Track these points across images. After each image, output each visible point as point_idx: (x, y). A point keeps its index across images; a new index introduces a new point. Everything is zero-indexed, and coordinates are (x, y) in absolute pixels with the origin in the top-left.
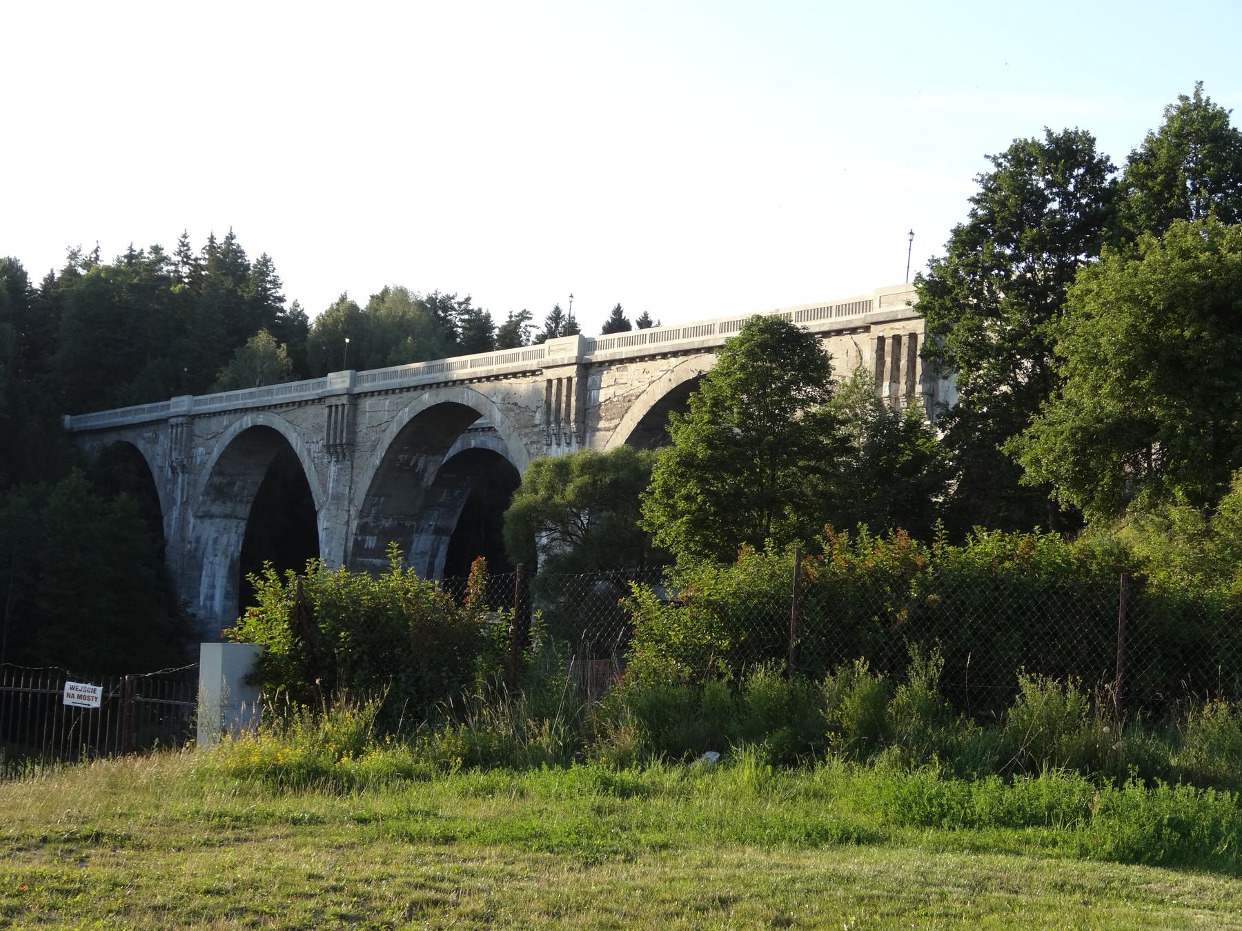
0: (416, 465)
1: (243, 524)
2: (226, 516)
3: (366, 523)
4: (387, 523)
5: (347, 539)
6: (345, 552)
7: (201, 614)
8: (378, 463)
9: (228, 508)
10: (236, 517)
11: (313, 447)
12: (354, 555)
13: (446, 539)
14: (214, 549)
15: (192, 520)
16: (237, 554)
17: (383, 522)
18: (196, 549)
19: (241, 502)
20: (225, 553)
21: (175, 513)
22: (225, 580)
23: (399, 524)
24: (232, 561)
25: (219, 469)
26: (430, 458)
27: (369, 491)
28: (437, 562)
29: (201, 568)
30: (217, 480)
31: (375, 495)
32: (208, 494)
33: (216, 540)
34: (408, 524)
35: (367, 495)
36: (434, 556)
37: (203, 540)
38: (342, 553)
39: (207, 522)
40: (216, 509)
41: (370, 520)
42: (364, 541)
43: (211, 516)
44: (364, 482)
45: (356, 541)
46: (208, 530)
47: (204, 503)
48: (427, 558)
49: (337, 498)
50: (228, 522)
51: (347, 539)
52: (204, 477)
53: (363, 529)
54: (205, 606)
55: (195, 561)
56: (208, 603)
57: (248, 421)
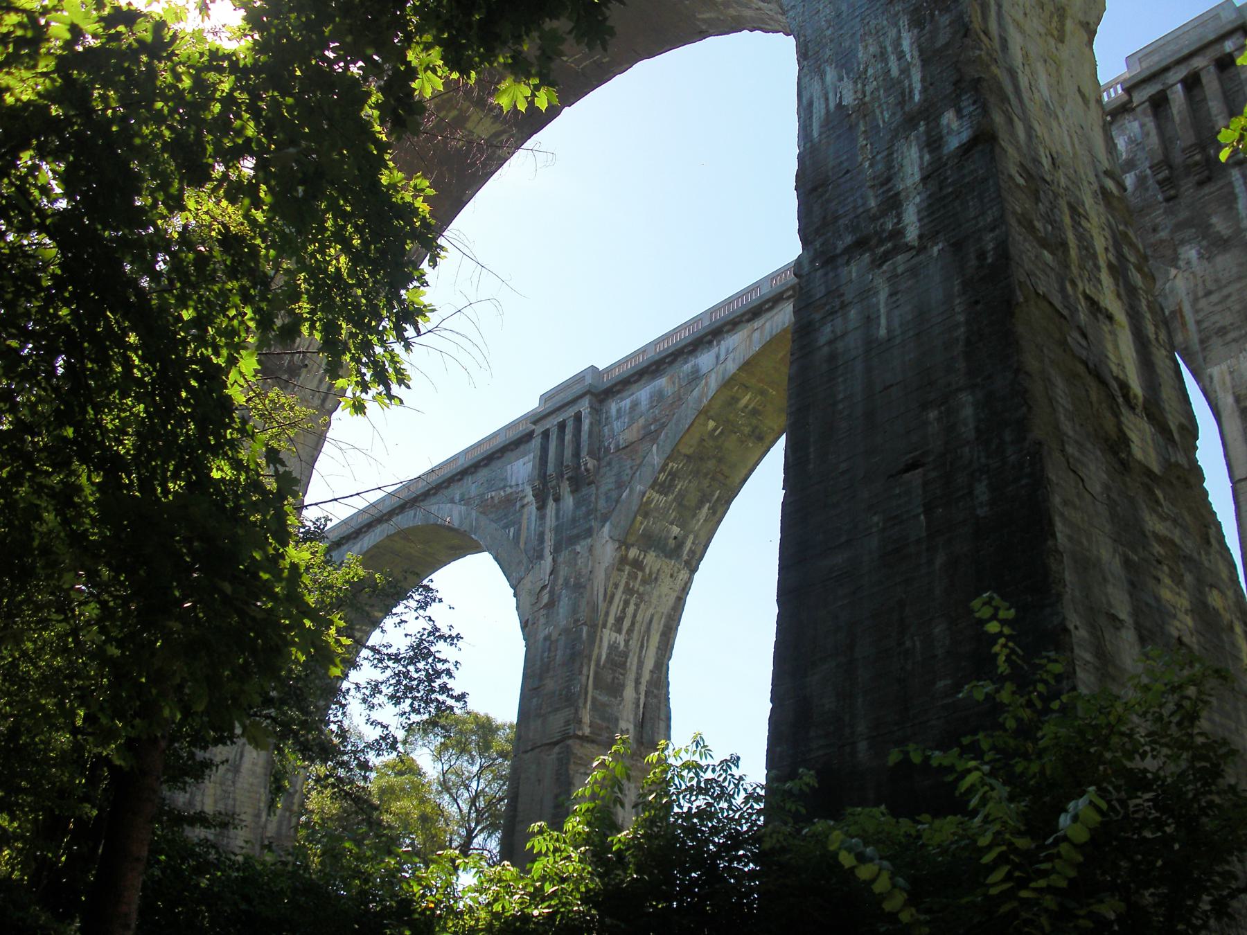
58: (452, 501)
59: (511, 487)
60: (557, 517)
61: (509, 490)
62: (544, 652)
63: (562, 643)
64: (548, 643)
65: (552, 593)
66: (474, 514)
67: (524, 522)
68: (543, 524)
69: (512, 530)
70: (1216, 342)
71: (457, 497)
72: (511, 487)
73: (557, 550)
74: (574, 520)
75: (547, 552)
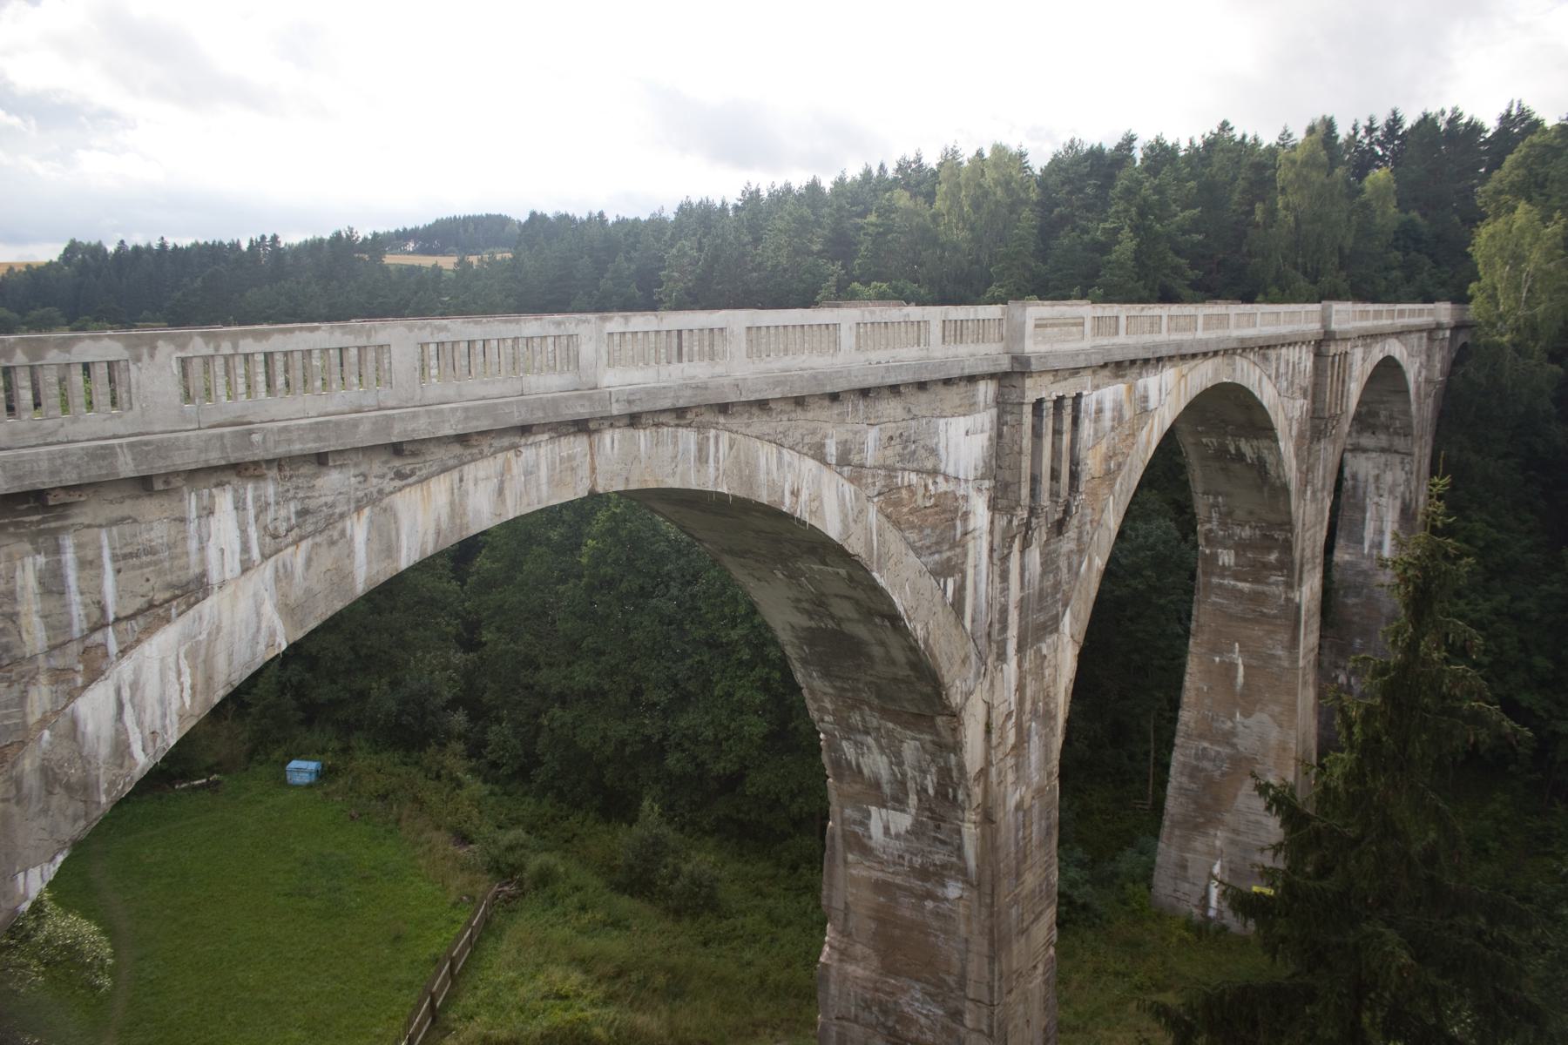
0: (1238, 449)
2: (1383, 450)
4: (1246, 533)
10: (1396, 452)
14: (1378, 488)
17: (1238, 530)
19: (1396, 433)
20: (1391, 492)
22: (1396, 526)
23: (1265, 536)
24: (1403, 502)
26: (1255, 443)
29: (1364, 511)
33: (1377, 478)
37: (1361, 476)
40: (1366, 440)
43: (1365, 450)
54: (1370, 556)
58: (819, 455)
59: (947, 478)
60: (1022, 588)
61: (943, 486)
62: (1017, 831)
63: (1036, 812)
64: (1021, 814)
65: (1019, 727)
66: (873, 515)
67: (970, 572)
68: (1005, 590)
69: (950, 582)
70: (1307, 568)
71: (832, 449)
72: (947, 478)
73: (1020, 649)
74: (1042, 596)
75: (1012, 647)
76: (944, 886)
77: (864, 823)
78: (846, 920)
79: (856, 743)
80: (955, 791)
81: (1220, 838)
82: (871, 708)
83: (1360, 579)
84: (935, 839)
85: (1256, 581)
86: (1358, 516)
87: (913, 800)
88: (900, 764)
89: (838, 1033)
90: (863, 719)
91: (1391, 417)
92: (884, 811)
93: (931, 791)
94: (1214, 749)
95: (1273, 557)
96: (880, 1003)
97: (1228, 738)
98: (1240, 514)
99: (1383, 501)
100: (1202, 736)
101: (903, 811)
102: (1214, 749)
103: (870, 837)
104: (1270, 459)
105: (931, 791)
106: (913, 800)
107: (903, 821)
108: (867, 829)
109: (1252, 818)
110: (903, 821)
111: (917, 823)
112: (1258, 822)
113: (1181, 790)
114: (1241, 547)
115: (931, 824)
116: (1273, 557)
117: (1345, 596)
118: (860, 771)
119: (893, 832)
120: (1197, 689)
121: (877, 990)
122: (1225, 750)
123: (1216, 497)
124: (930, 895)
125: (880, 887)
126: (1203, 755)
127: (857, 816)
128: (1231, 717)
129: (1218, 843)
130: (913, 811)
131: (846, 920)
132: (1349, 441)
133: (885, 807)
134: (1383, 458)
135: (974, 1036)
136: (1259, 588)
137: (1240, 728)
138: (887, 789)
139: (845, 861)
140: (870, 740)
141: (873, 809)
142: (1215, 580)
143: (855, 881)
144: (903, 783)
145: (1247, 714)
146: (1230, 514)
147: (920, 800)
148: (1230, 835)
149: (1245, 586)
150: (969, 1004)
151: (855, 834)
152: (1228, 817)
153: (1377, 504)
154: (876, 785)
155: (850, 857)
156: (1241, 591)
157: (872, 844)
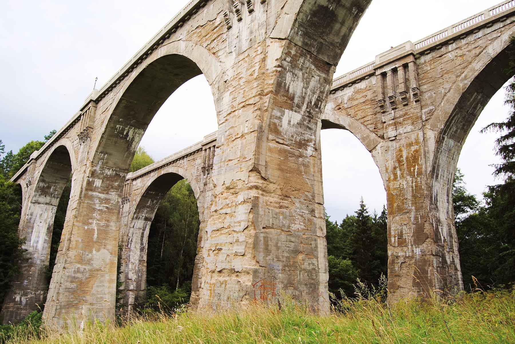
0: (127, 135)
1: (55, 209)
2: (46, 204)
3: (95, 170)
4: (109, 172)
5: (83, 180)
6: (82, 188)
7: (31, 250)
8: (103, 129)
9: (48, 199)
10: (51, 205)
11: (75, 142)
12: (87, 190)
13: (149, 223)
15: (30, 204)
16: (52, 222)
18: (30, 219)
19: (54, 197)
20: (46, 220)
21: (25, 204)
23: (116, 174)
25: (42, 179)
27: (98, 149)
28: (145, 233)
29: (33, 228)
30: (42, 184)
31: (101, 153)
32: (38, 192)
34: (122, 174)
35: (97, 151)
36: (144, 230)
37: (34, 214)
38: (80, 189)
39: (37, 205)
40: (42, 199)
41: (98, 168)
42: (93, 182)
43: (39, 203)
44: (95, 144)
45: (88, 181)
46: (38, 209)
47: (35, 196)
48: (141, 231)
49: (81, 161)
50: (48, 206)
51: (83, 180)
52: (35, 185)
53: (93, 174)
55: (30, 224)
56: (35, 245)
57: (53, 149)
76: (307, 150)
77: (280, 118)
78: (266, 171)
79: (293, 74)
80: (321, 104)
81: (84, 309)
82: (311, 57)
83: (28, 256)
84: (307, 127)
85: (107, 193)
86: (30, 231)
87: (304, 108)
88: (306, 88)
89: (265, 238)
90: (304, 63)
91: (55, 190)
92: (291, 112)
93: (313, 103)
94: (82, 267)
95: (116, 184)
96: (283, 214)
97: (89, 262)
98: (111, 164)
99: (41, 224)
100: (79, 263)
101: (299, 112)
102: (82, 267)
103: (281, 126)
104: (136, 139)
105: (313, 103)
106: (304, 108)
107: (297, 117)
108: (281, 121)
109: (99, 296)
110: (297, 117)
111: (303, 119)
112: (101, 298)
113: (67, 289)
114: (106, 178)
115: (308, 119)
116: (116, 184)
117: (21, 263)
118: (288, 91)
119: (292, 123)
120: (77, 241)
121: (281, 207)
122: (88, 267)
123: (105, 155)
124: (301, 156)
125: (281, 152)
126: (78, 271)
127: (279, 114)
128: (91, 252)
129: (83, 311)
130: (302, 113)
131: (266, 171)
132: (34, 199)
133: (292, 110)
134: (46, 206)
135: (319, 220)
136: (107, 196)
137: (95, 257)
138: (296, 101)
139: (268, 139)
140: (300, 74)
141: (287, 111)
142: (90, 193)
143: (270, 150)
144: (304, 98)
145: (98, 250)
146: (107, 163)
147: (307, 108)
148: (89, 306)
149: (102, 196)
150: (316, 205)
151: (275, 124)
152: (88, 298)
153: (39, 226)
154: (292, 99)
155: (271, 137)
156: (100, 198)
157: (281, 129)
